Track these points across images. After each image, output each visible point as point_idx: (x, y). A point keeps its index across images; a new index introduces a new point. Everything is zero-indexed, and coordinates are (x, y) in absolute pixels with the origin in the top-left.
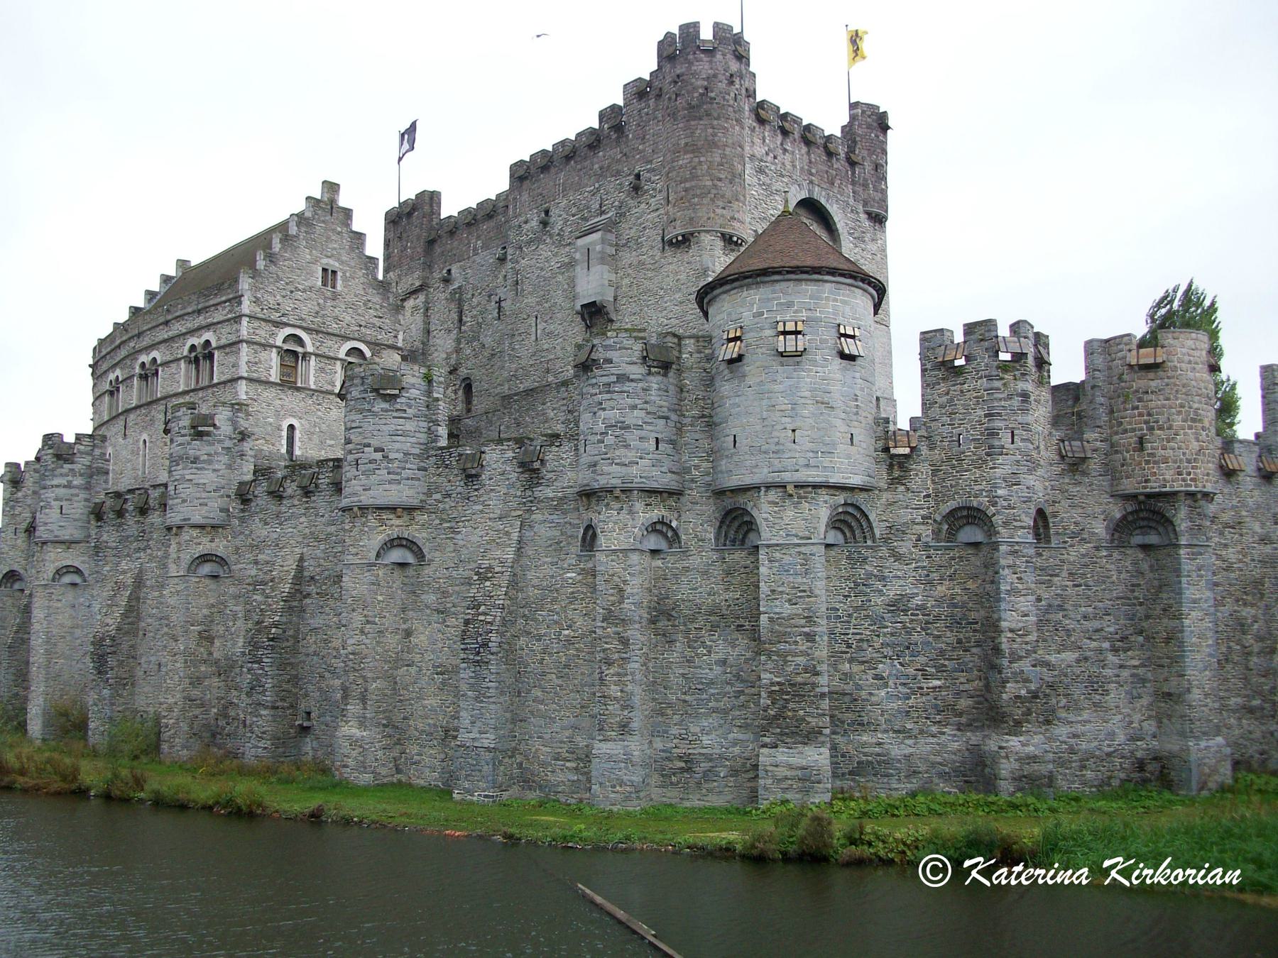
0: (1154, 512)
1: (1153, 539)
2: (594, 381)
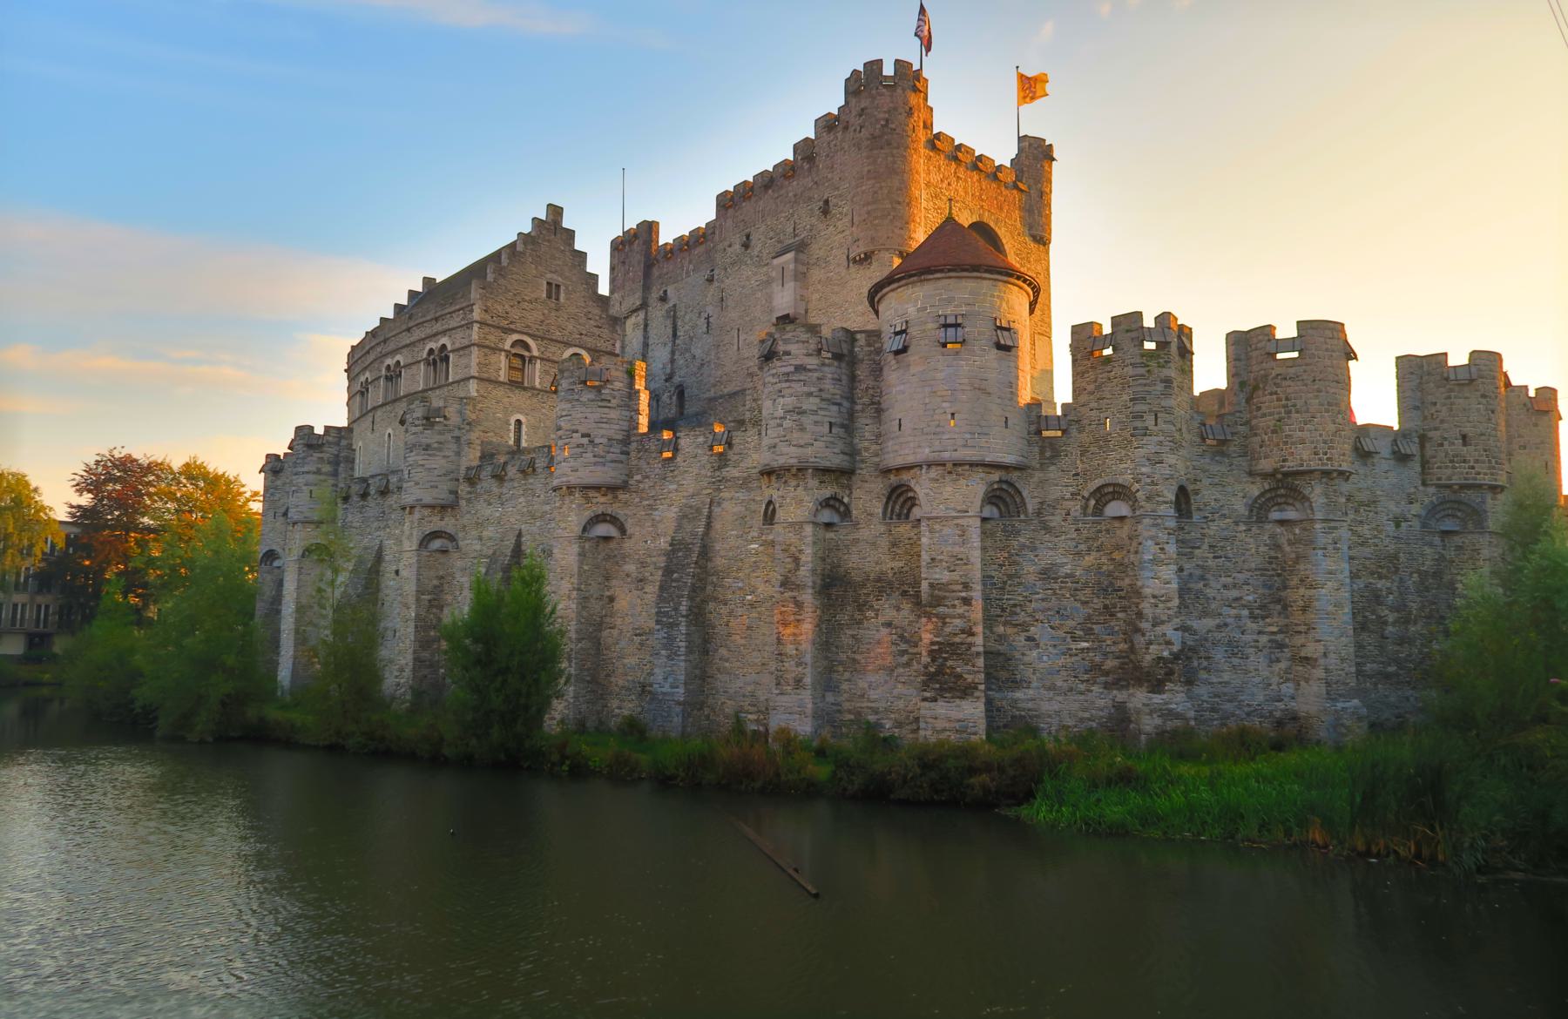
1: (1291, 514)
2: (774, 371)
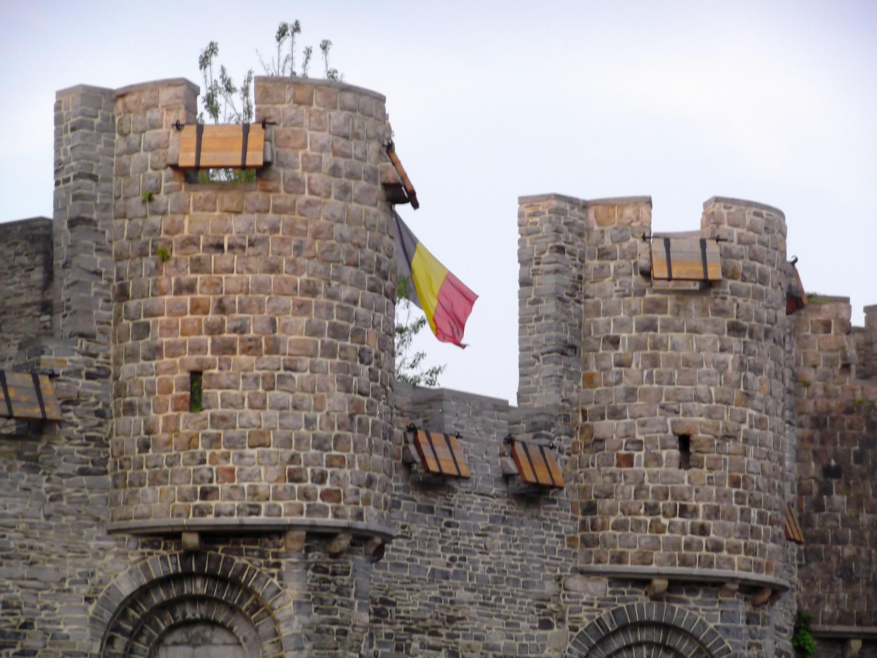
0: (223, 580)
